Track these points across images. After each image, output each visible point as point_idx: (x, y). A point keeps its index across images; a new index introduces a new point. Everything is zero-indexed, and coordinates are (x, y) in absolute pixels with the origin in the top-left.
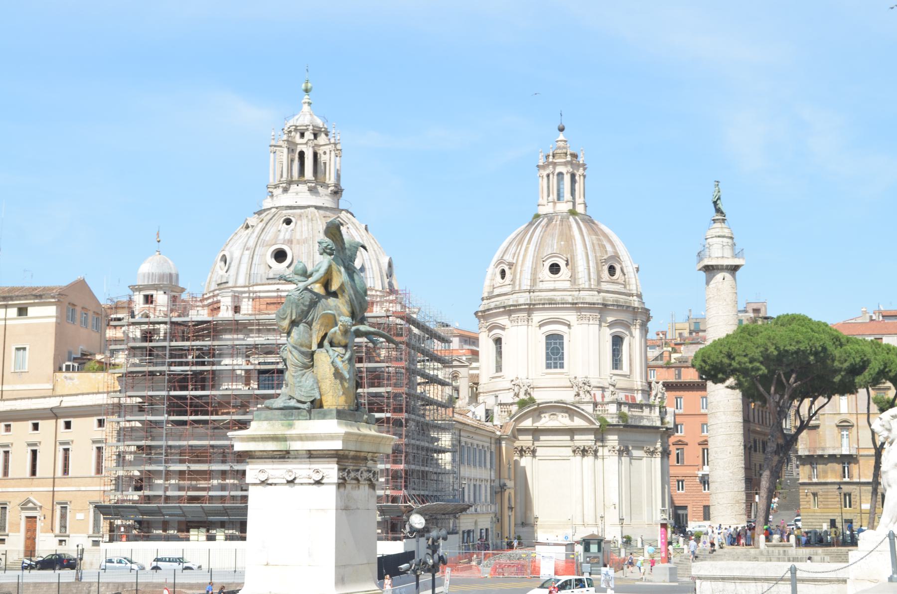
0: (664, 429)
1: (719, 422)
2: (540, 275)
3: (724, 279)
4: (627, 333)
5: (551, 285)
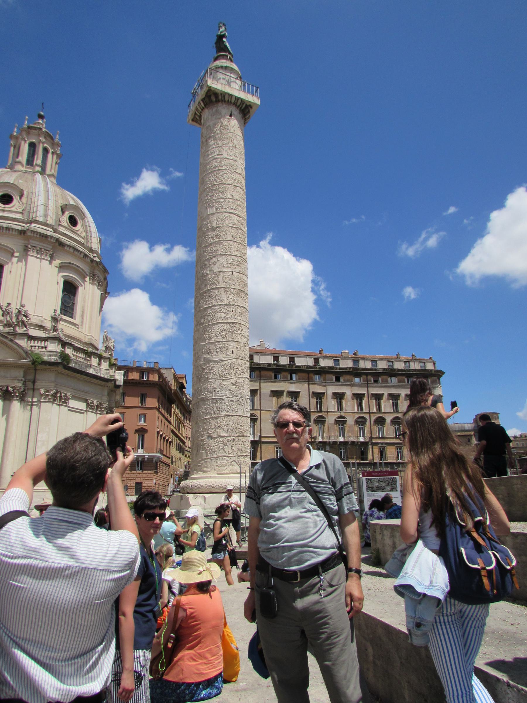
1: (216, 304)
4: (82, 284)
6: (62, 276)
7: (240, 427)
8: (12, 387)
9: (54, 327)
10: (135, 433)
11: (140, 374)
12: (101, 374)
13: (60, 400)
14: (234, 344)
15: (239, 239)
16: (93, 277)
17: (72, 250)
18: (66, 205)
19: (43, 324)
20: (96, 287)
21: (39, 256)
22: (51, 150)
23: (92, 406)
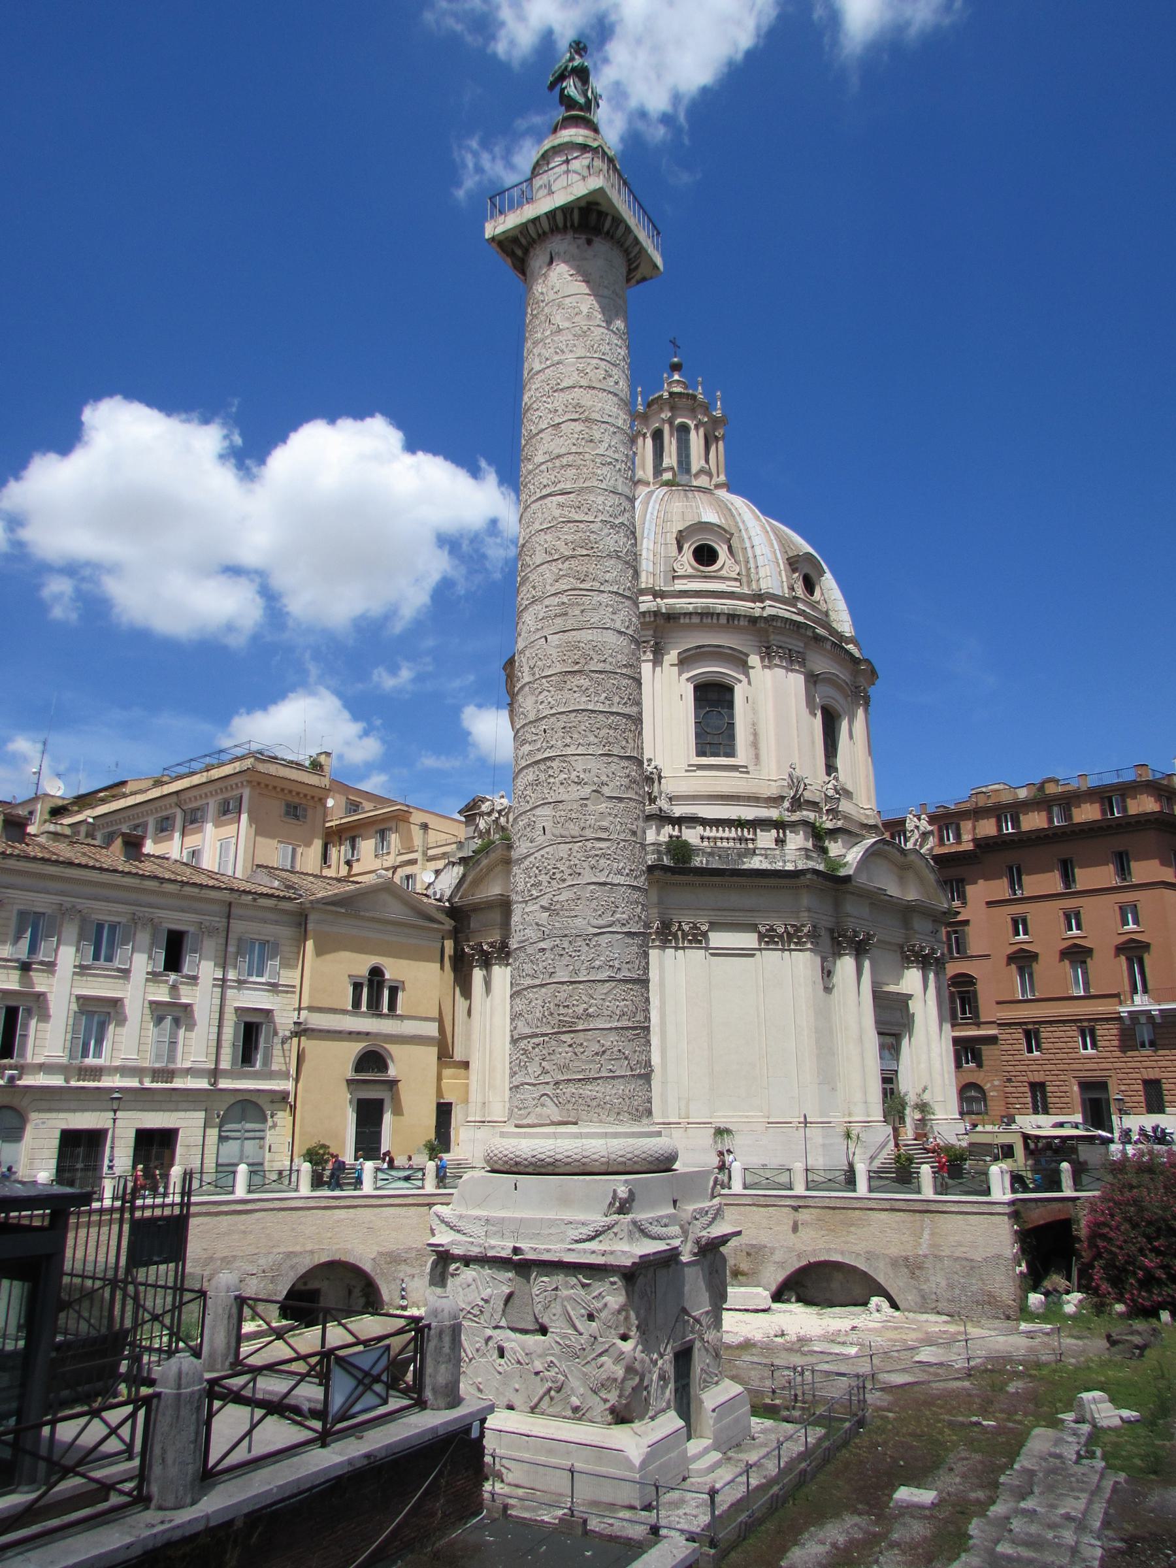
4: (741, 677)
6: (688, 680)
7: (562, 1011)
9: (650, 794)
10: (1117, 955)
11: (1102, 805)
12: (785, 862)
13: (683, 939)
14: (547, 811)
16: (768, 654)
17: (696, 620)
18: (680, 531)
20: (780, 672)
22: (691, 424)
23: (772, 937)
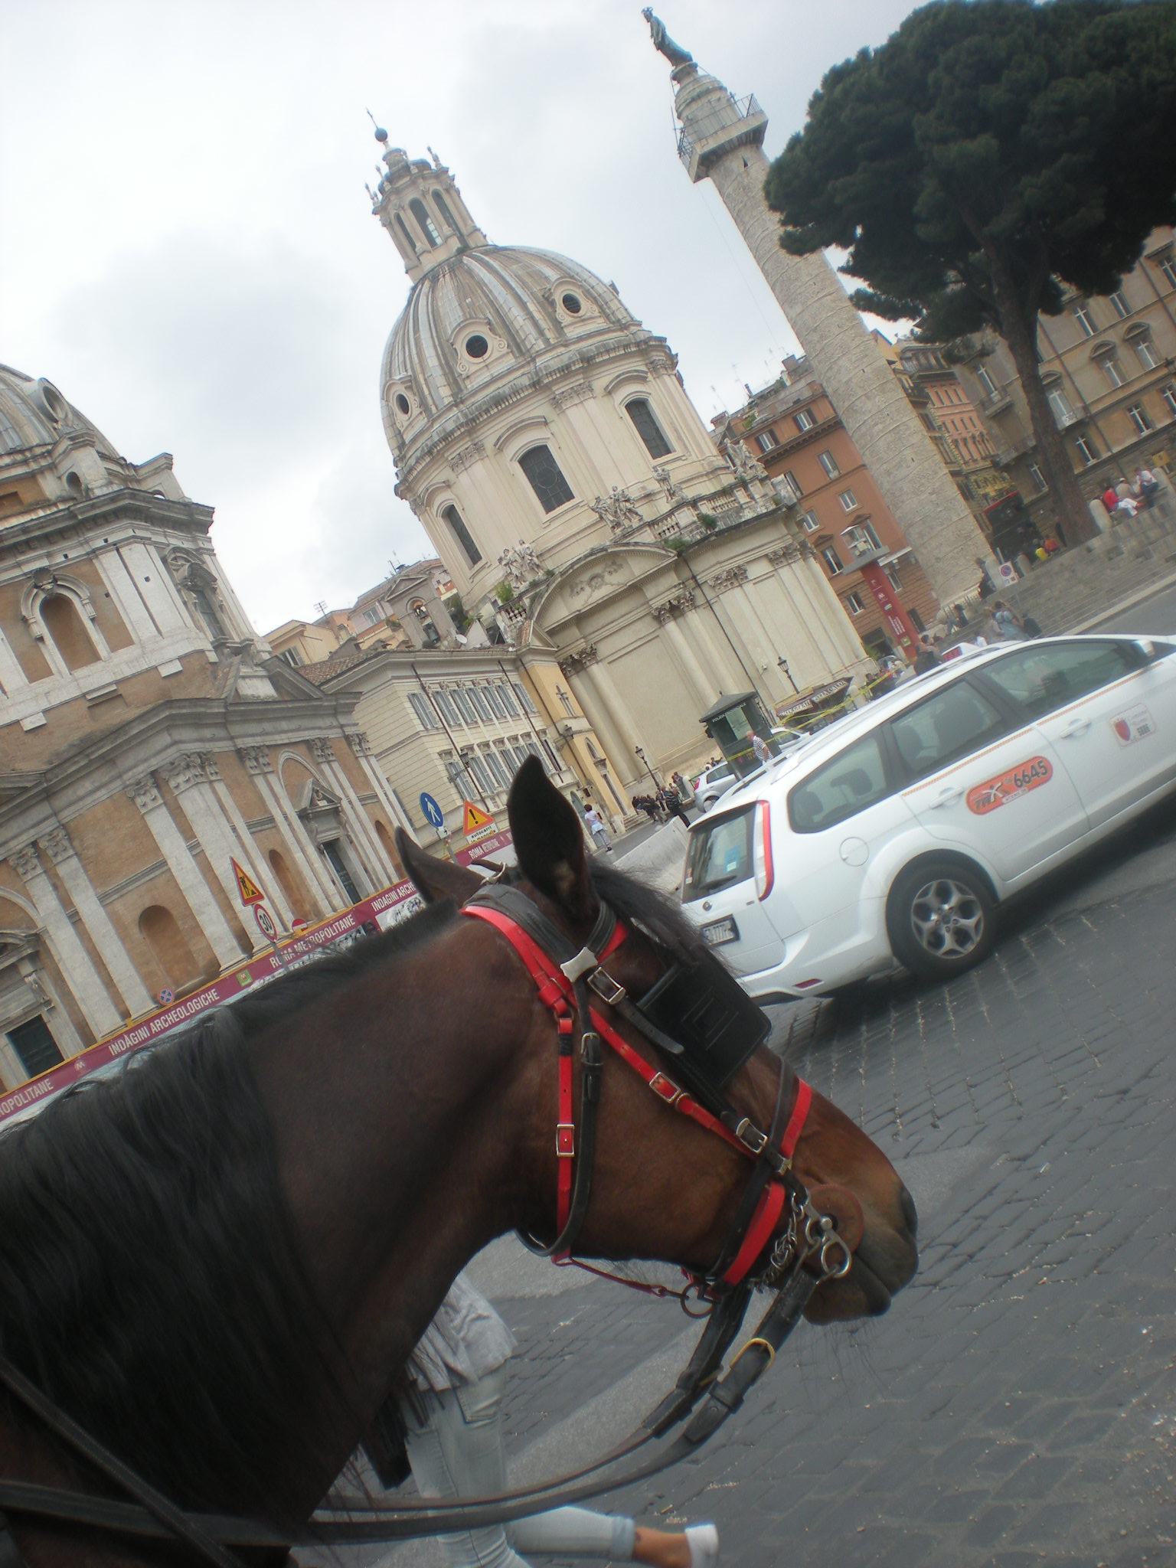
0: (784, 509)
2: (459, 369)
3: (746, 165)
5: (485, 377)
8: (675, 599)
15: (847, 323)
16: (654, 367)
19: (647, 492)
21: (577, 402)
